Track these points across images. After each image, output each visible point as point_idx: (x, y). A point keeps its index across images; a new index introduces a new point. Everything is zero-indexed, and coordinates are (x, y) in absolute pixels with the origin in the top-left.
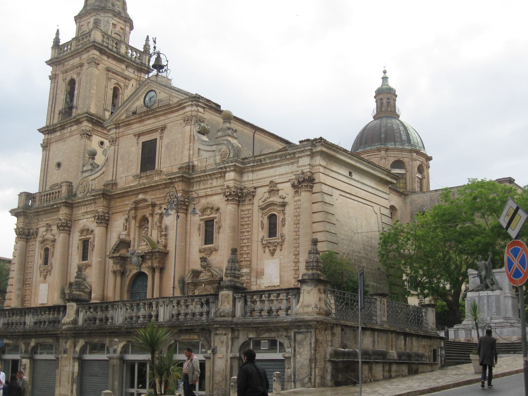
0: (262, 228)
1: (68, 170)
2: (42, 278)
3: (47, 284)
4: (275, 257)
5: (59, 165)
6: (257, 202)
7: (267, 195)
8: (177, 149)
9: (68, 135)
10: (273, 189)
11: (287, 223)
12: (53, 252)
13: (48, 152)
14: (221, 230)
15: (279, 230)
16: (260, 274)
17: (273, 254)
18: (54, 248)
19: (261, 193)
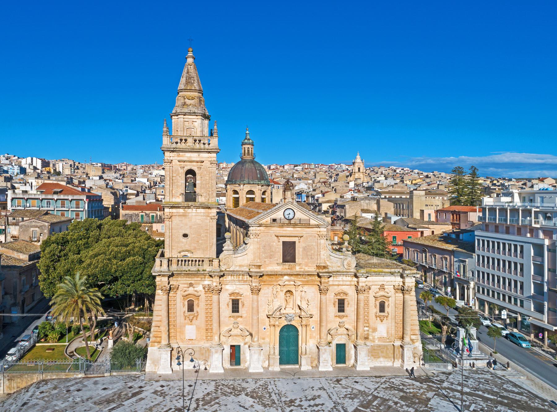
0: (375, 307)
1: (198, 242)
2: (187, 321)
3: (195, 326)
4: (383, 323)
5: (185, 236)
6: (372, 293)
7: (378, 290)
8: (312, 252)
9: (194, 214)
10: (382, 287)
11: (390, 306)
12: (198, 303)
13: (170, 222)
14: (349, 305)
15: (386, 309)
16: (375, 330)
17: (382, 321)
18: (198, 301)
19: (374, 288)
